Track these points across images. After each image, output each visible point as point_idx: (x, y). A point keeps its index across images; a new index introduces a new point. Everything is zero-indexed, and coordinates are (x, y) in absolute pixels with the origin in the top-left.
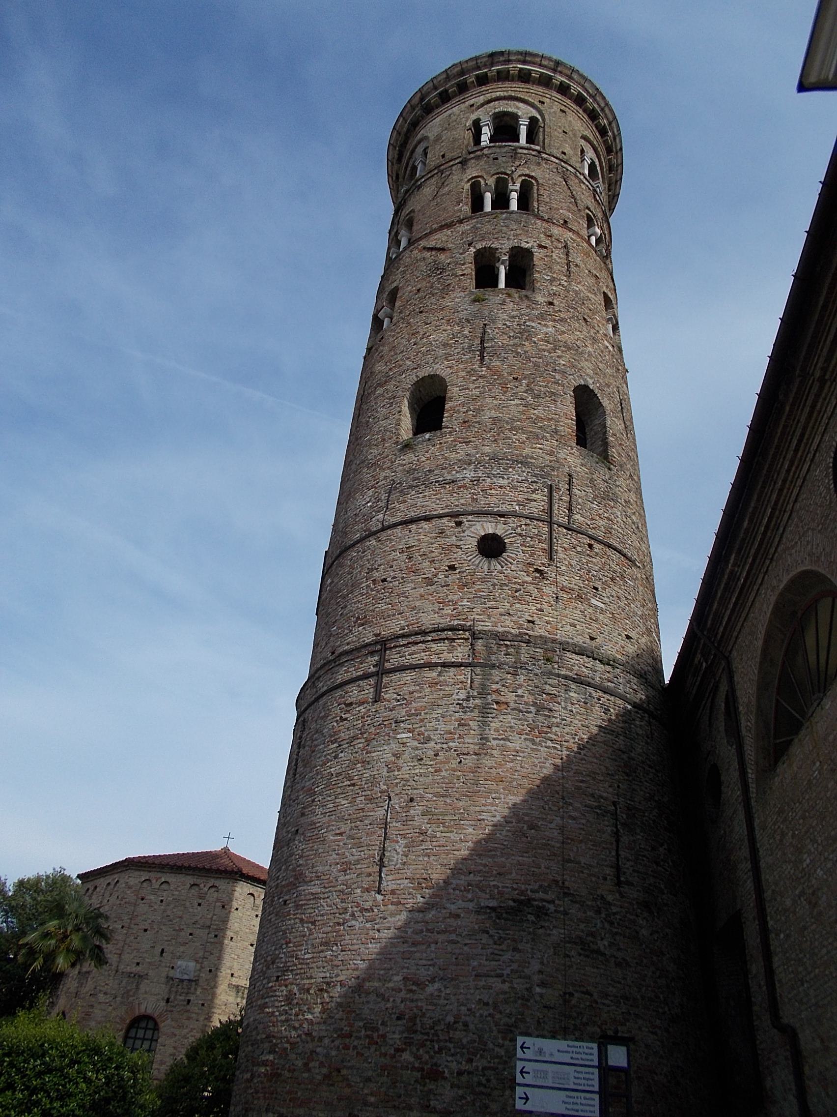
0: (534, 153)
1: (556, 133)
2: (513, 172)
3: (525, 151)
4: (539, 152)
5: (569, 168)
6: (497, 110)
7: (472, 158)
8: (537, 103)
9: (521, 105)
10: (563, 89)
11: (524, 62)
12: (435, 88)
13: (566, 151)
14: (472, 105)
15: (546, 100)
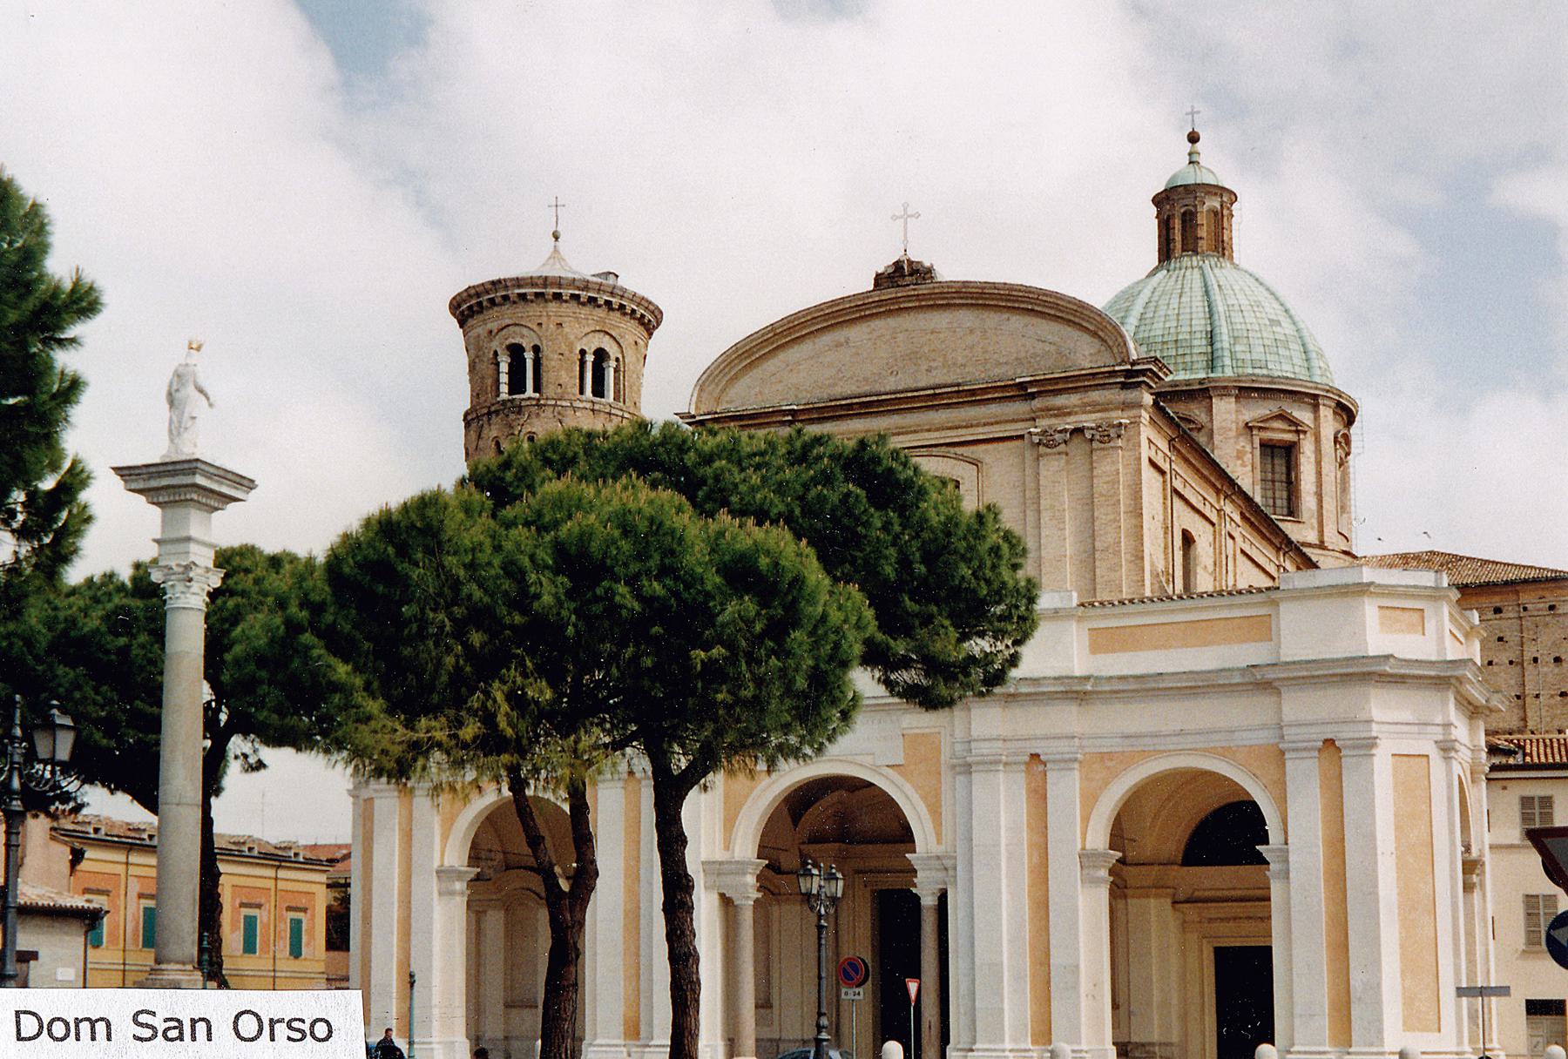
0: (534, 403)
1: (553, 363)
2: (520, 431)
3: (528, 403)
4: (538, 400)
5: (564, 403)
6: (508, 342)
7: (494, 412)
8: (535, 328)
9: (525, 331)
10: (558, 297)
11: (519, 287)
12: (465, 301)
13: (561, 382)
14: (491, 332)
15: (544, 320)
